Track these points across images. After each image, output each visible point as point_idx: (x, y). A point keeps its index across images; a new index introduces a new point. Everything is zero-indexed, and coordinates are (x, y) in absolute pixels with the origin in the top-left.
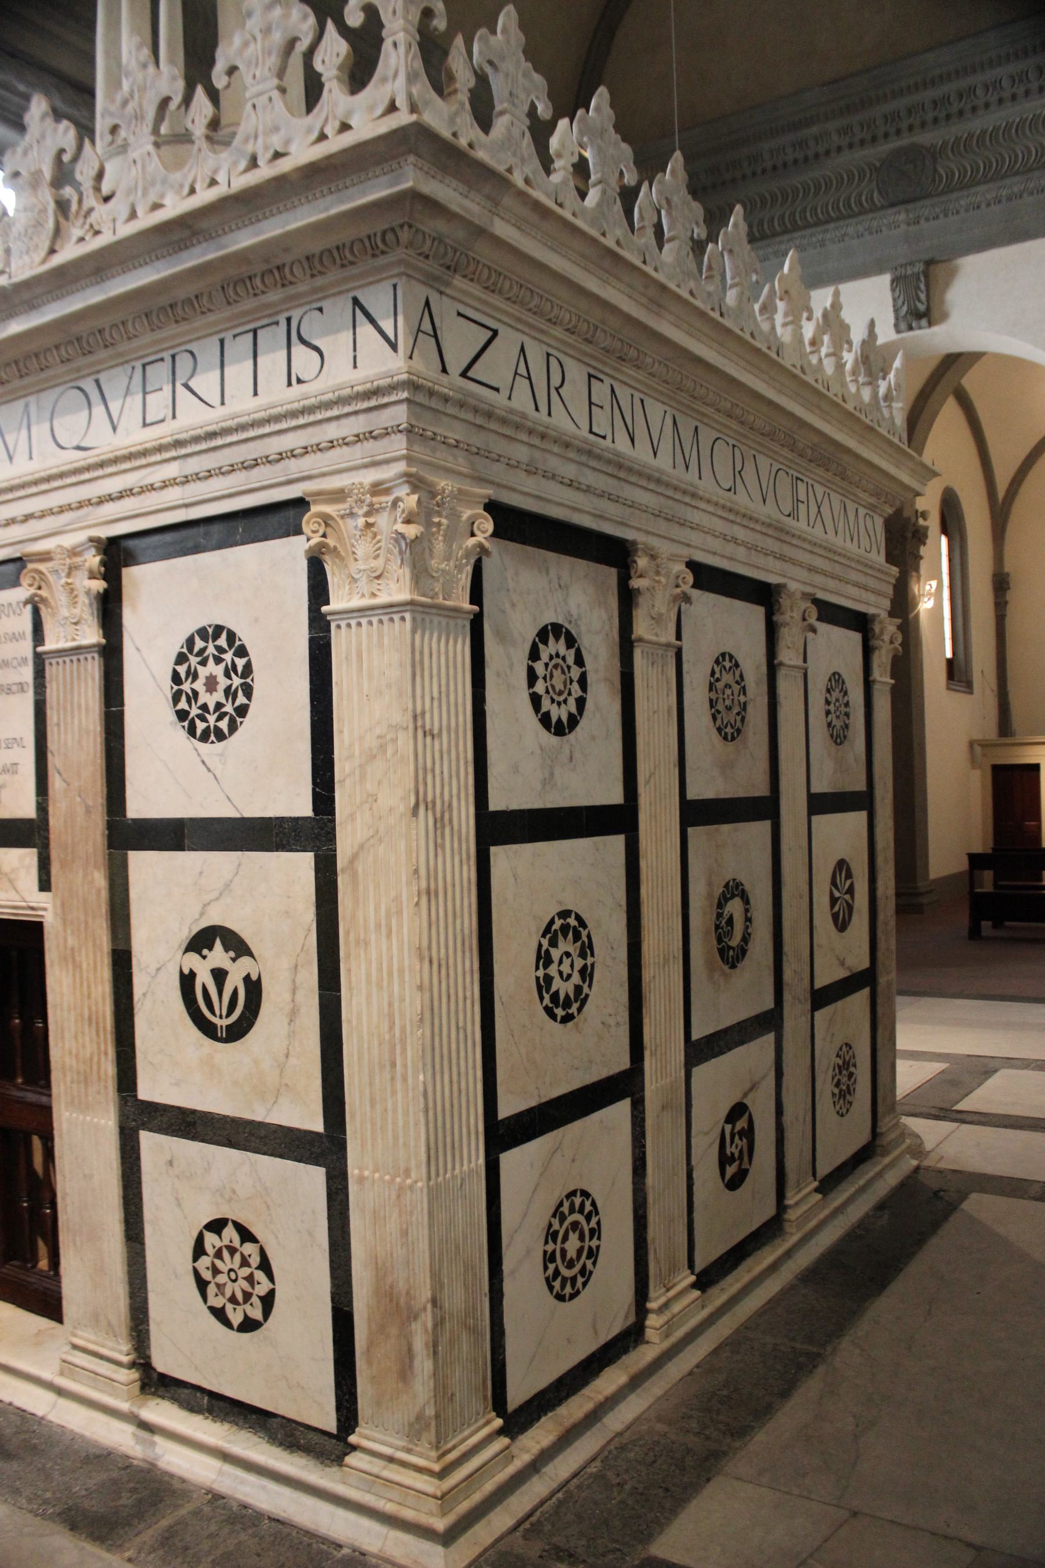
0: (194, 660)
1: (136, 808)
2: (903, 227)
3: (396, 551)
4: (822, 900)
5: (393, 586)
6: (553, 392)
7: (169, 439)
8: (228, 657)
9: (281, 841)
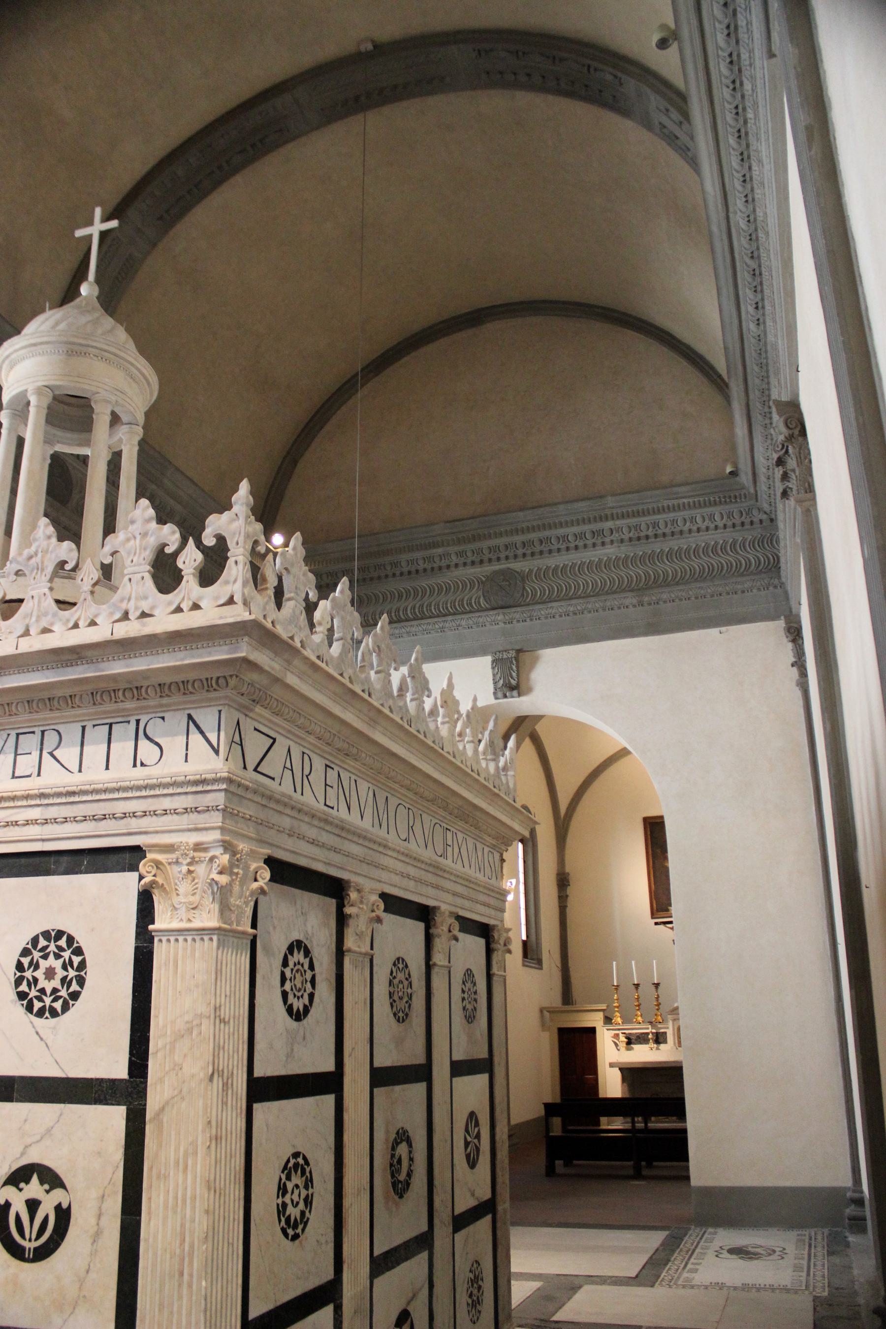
0: (36, 955)
2: (502, 625)
3: (210, 892)
4: (459, 1144)
5: (205, 915)
6: (305, 778)
7: (36, 792)
8: (66, 955)
9: (99, 1096)
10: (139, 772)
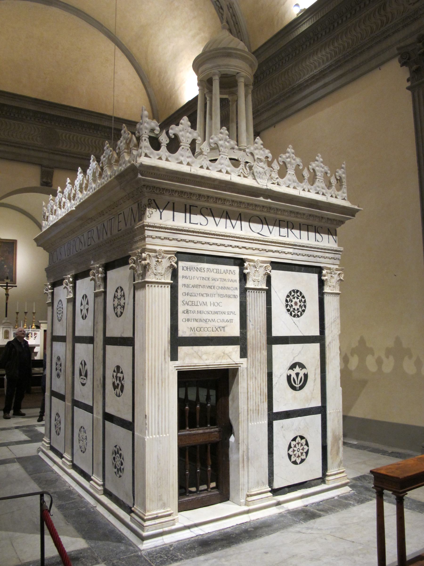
0: (291, 297)
1: (275, 333)
8: (300, 298)
10: (317, 243)
